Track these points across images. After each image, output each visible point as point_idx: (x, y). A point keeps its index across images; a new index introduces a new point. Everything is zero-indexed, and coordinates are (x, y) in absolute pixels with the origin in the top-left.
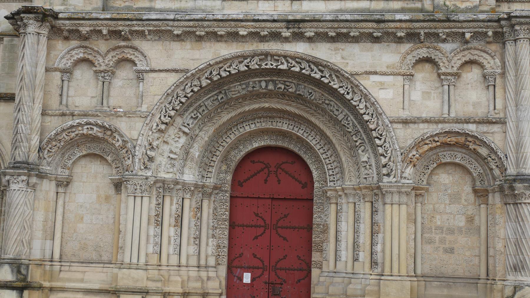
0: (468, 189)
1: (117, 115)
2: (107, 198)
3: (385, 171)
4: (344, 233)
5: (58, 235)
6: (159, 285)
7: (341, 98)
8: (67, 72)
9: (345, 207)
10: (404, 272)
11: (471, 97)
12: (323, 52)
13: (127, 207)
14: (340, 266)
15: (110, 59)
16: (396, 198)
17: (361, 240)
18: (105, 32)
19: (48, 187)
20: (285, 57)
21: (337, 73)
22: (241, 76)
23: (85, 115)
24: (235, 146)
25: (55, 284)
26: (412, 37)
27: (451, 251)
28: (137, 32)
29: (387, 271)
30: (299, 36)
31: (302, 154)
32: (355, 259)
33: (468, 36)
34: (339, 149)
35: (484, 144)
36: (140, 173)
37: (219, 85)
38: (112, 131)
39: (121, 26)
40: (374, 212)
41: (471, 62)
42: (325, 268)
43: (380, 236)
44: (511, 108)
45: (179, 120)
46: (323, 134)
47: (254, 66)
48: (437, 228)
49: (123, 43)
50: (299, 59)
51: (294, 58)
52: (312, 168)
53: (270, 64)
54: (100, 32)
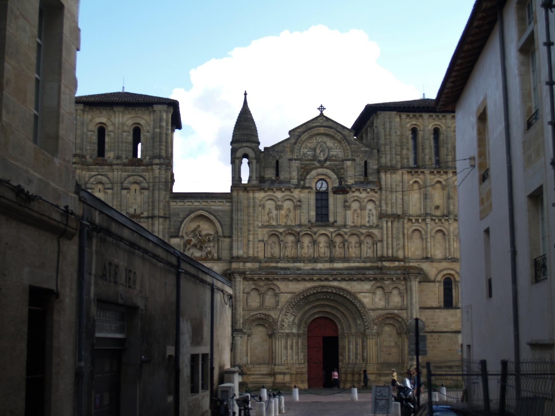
0: (395, 332)
1: (270, 310)
2: (266, 340)
3: (367, 327)
4: (351, 349)
5: (249, 355)
6: (289, 371)
7: (351, 301)
8: (248, 293)
9: (351, 339)
10: (374, 362)
11: (396, 299)
12: (344, 285)
13: (275, 344)
14: (351, 361)
15: (265, 288)
16: (371, 337)
17: (358, 352)
18: (263, 279)
19: (245, 337)
20: (330, 287)
21: (349, 293)
22: (314, 294)
23: (257, 310)
24: (309, 318)
25: (251, 373)
26: (375, 279)
27: (390, 354)
28: (276, 279)
29: (369, 362)
30: (335, 280)
31: (334, 319)
32: (356, 358)
33: (394, 279)
34: (349, 318)
35: (400, 317)
36: (280, 331)
37: (305, 298)
38: (269, 316)
39: (270, 276)
40: (363, 342)
41: (396, 288)
42: (344, 362)
43: (366, 350)
44: (409, 305)
45: (291, 310)
46: (342, 313)
47: (319, 290)
48: (385, 346)
49: (270, 283)
50: (335, 288)
51: (333, 287)
52: (338, 324)
53: (325, 290)
54: (262, 279)
